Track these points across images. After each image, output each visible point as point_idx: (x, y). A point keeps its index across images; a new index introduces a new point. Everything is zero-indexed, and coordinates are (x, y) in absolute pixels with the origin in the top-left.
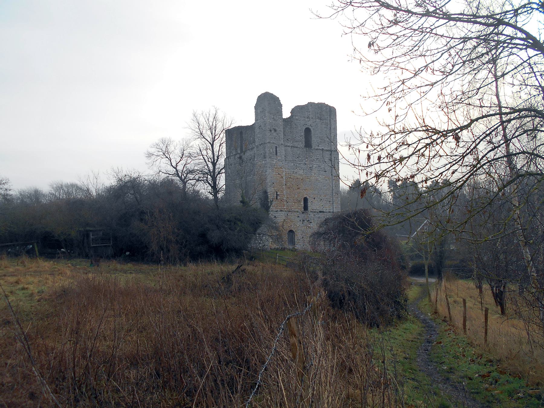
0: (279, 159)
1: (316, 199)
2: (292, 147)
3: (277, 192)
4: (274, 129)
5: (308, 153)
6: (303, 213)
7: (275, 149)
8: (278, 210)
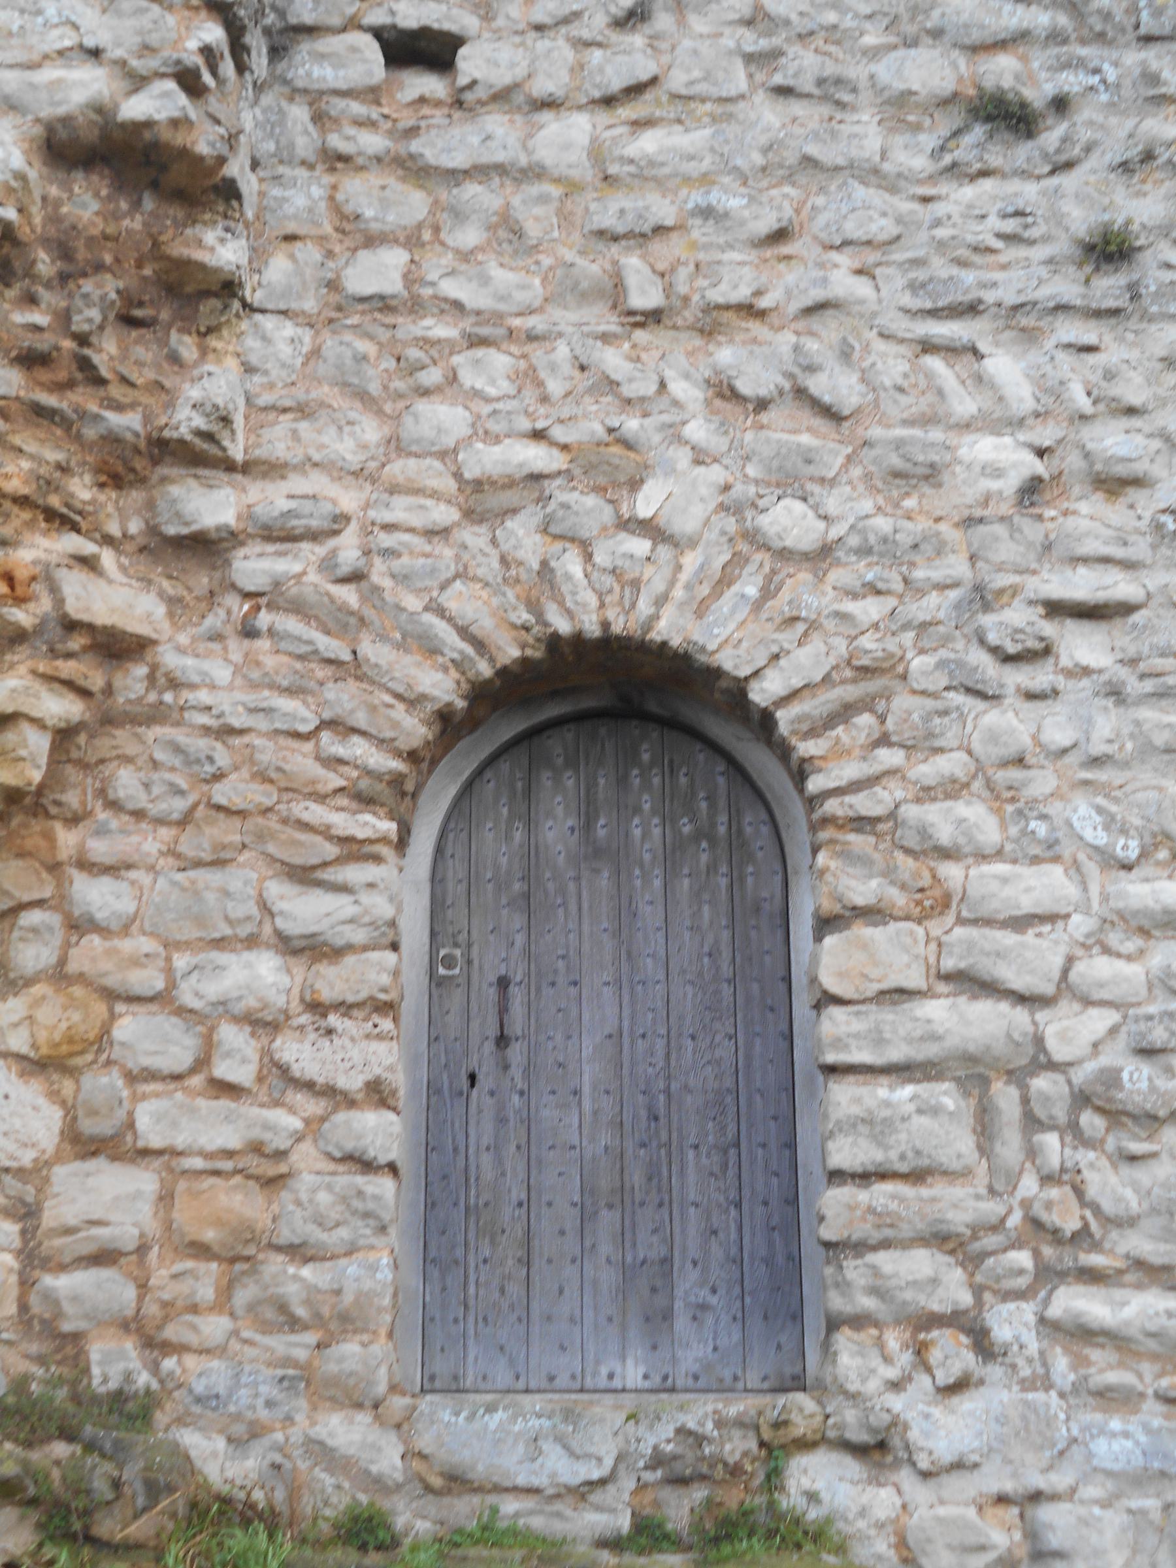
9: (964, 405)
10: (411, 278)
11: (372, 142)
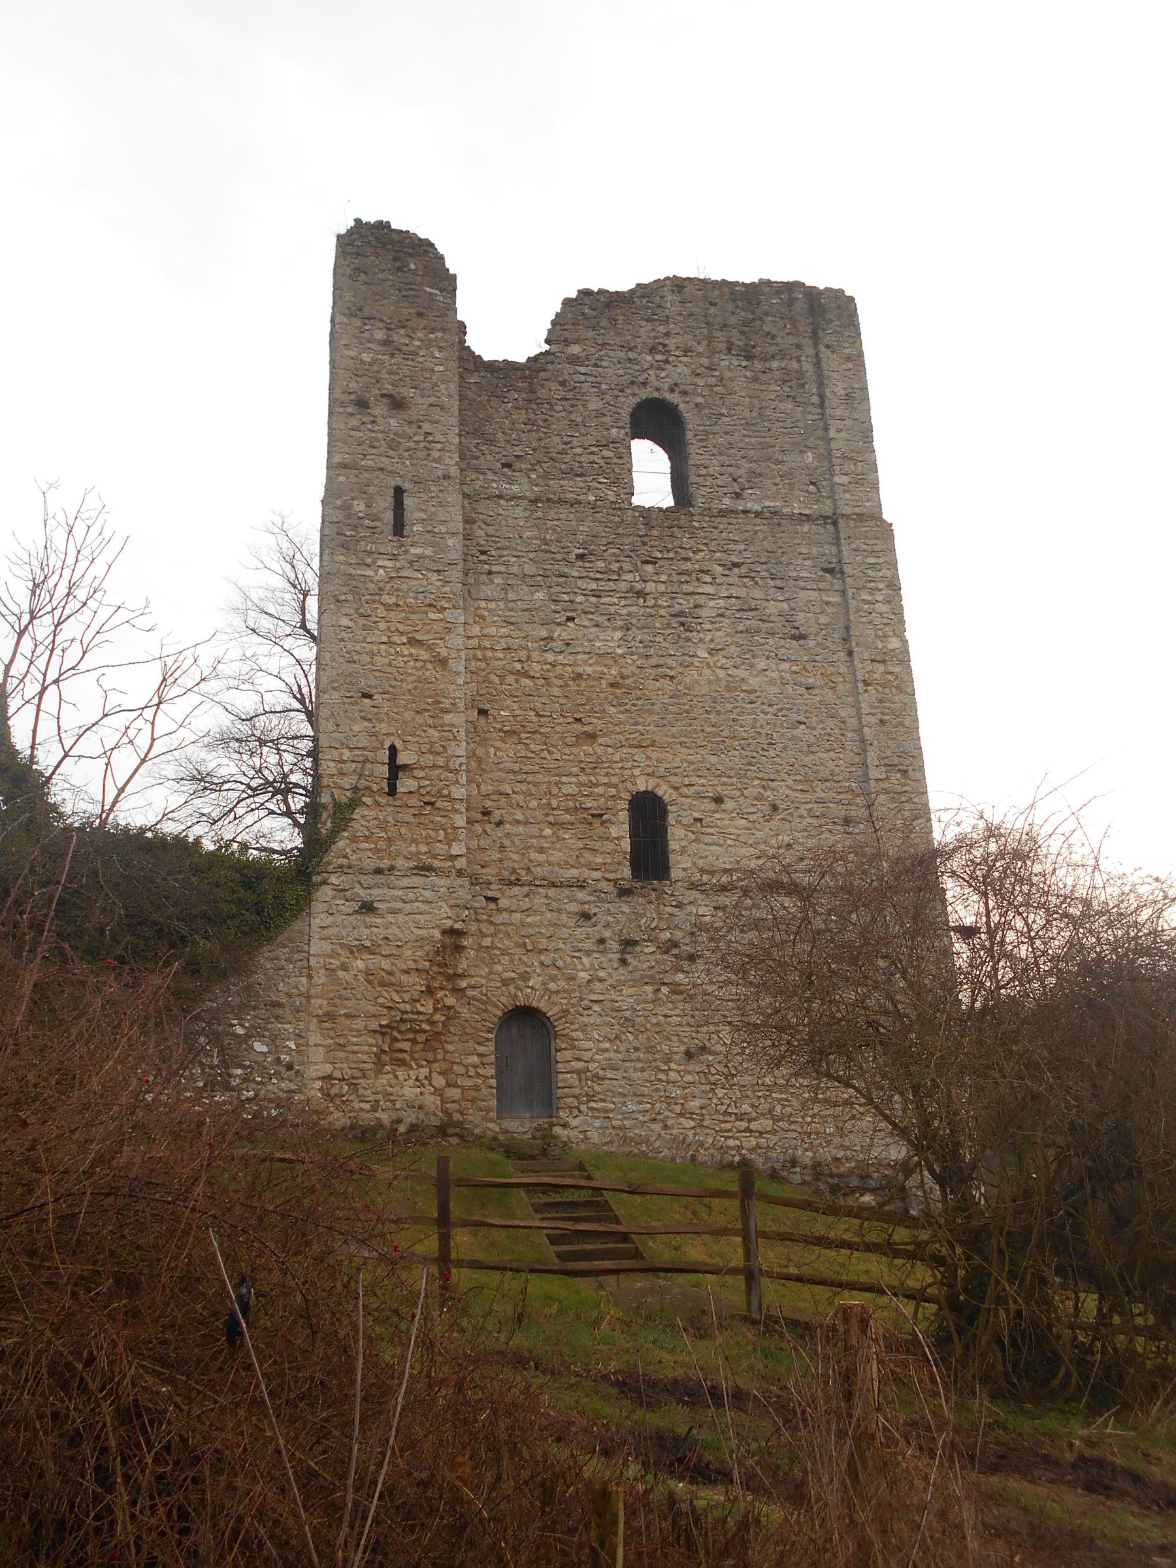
0: (420, 557)
1: (729, 805)
2: (534, 502)
3: (393, 750)
4: (389, 396)
5: (655, 532)
6: (624, 893)
7: (385, 503)
8: (401, 863)
9: (580, 967)
10: (492, 943)
11: (485, 917)
